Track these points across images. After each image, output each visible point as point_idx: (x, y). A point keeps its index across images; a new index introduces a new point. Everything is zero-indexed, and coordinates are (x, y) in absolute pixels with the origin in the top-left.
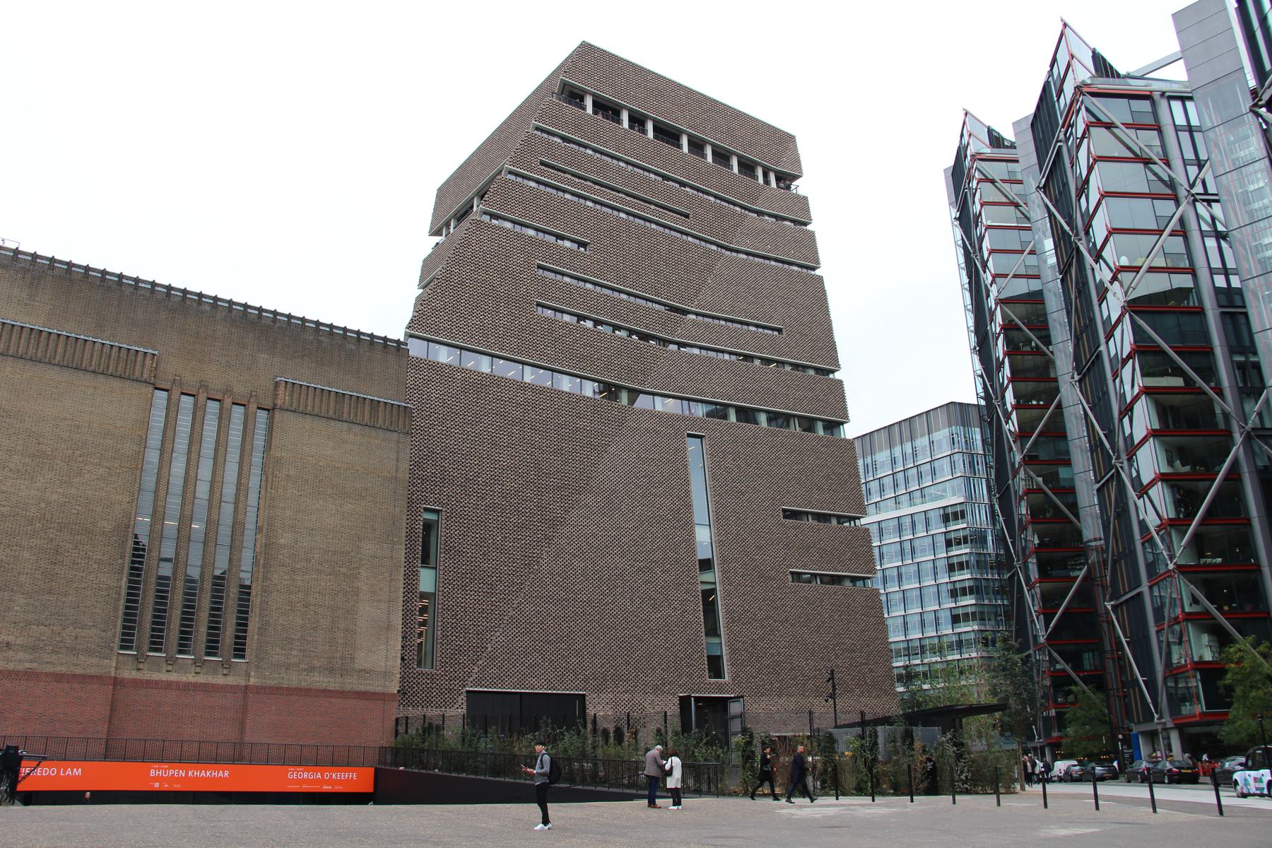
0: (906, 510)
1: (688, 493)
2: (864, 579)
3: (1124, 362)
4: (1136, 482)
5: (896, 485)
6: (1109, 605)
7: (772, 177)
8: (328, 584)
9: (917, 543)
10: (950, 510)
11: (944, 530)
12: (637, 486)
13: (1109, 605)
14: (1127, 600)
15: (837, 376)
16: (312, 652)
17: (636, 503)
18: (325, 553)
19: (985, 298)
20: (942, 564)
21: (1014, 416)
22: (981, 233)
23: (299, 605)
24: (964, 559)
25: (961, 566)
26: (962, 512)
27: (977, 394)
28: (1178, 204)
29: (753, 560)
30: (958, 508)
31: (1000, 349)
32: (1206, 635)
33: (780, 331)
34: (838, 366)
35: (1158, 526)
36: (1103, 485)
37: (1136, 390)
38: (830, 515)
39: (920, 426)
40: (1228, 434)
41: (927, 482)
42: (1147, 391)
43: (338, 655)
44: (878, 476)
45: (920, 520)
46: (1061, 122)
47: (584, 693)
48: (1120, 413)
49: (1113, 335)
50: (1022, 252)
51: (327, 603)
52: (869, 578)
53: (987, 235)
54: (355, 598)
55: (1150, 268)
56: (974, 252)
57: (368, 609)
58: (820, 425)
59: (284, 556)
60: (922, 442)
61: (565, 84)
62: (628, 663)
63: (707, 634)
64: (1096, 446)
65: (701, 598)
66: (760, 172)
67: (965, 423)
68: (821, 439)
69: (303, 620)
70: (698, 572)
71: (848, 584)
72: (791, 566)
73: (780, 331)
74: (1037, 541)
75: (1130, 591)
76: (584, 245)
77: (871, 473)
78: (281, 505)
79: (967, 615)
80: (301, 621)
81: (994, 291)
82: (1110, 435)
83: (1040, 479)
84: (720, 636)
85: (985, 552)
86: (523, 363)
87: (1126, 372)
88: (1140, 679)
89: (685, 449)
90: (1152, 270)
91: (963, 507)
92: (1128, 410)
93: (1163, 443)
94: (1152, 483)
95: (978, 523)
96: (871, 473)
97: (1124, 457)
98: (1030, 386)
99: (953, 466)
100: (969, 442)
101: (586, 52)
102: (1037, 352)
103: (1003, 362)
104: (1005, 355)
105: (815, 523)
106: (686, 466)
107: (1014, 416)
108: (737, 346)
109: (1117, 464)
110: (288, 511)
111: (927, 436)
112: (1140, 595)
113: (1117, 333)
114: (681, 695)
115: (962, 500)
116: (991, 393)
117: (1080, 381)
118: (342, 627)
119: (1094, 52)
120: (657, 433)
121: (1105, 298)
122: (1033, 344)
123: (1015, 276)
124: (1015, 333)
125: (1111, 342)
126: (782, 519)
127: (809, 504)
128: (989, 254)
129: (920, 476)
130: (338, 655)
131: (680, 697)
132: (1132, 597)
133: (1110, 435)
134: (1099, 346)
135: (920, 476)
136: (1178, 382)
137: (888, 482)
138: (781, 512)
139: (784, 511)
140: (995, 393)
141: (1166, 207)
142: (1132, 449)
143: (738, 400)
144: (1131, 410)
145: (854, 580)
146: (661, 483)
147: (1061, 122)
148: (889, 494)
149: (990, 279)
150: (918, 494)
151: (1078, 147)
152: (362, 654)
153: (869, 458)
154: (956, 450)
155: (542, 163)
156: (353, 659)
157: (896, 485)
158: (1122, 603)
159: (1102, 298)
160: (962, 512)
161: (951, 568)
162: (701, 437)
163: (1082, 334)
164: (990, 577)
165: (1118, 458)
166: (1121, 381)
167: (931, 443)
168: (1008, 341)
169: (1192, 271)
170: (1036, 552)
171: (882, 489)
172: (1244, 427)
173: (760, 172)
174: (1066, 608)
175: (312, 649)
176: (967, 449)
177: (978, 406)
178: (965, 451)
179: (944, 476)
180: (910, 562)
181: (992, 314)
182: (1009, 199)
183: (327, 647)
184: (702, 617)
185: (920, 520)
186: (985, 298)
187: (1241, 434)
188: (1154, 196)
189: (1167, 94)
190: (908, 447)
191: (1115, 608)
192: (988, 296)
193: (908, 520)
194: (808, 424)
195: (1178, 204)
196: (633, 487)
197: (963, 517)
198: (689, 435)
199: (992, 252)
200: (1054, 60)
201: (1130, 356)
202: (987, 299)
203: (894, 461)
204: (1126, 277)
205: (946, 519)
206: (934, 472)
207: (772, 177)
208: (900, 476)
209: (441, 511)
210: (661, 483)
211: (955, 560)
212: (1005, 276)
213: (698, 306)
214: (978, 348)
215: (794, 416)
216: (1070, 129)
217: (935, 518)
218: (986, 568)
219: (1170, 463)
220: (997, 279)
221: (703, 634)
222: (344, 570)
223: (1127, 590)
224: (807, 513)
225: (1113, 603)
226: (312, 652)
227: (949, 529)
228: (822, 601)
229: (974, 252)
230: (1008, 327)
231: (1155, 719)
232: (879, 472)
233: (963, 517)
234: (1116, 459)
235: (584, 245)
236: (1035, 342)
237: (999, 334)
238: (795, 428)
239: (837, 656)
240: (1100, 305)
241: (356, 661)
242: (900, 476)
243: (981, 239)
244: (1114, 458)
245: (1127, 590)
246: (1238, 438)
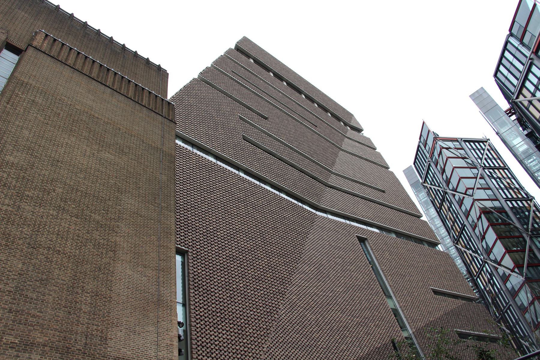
8: (73, 227)
16: (34, 316)
18: (72, 191)
23: (21, 242)
43: (80, 329)
51: (67, 250)
54: (111, 254)
57: (129, 272)
59: (9, 175)
69: (24, 264)
78: (17, 123)
80: (20, 266)
101: (245, 40)
110: (26, 133)
118: (89, 287)
130: (80, 329)
152: (119, 334)
155: (232, 71)
156: (104, 340)
175: (32, 312)
183: (61, 314)
209: (187, 251)
222: (98, 217)
226: (34, 316)
241: (111, 343)
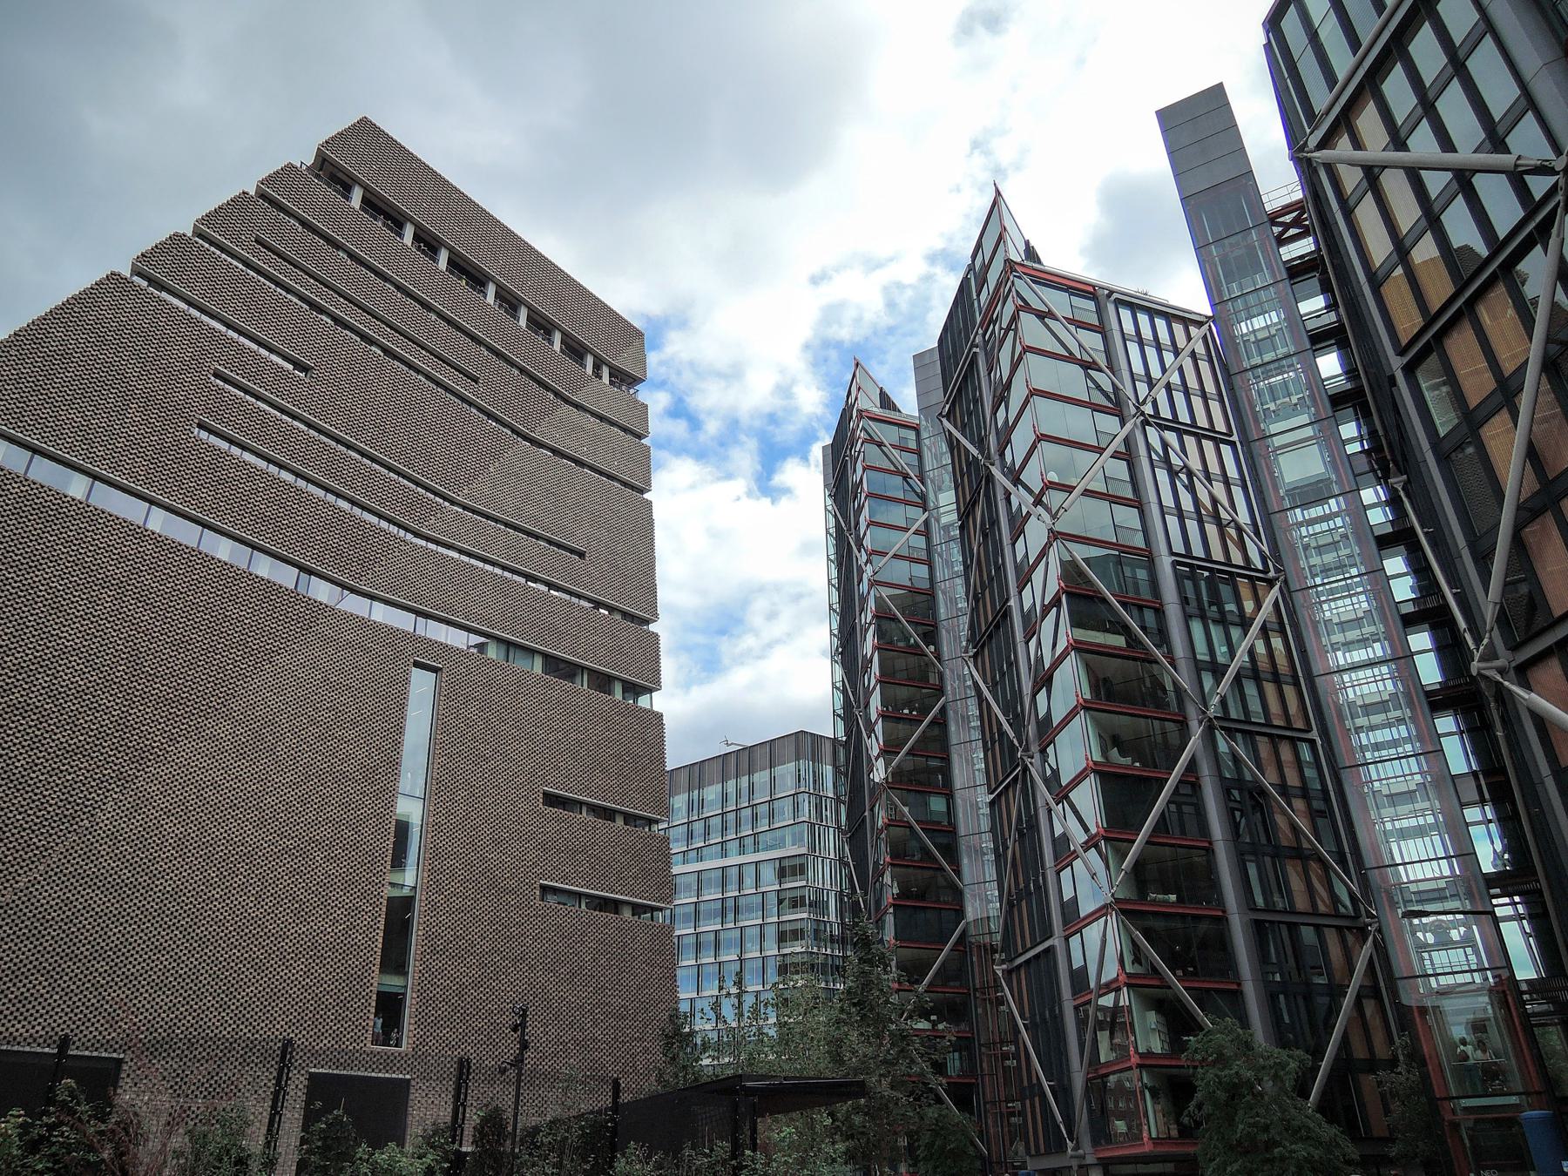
0: (734, 859)
1: (397, 744)
2: (653, 909)
3: (1046, 610)
4: (1053, 780)
5: (724, 829)
6: (999, 970)
7: (605, 372)
9: (742, 901)
10: (786, 863)
11: (777, 887)
12: (313, 721)
13: (999, 970)
14: (1028, 962)
15: (653, 627)
17: (305, 746)
19: (856, 583)
20: (771, 932)
21: (879, 728)
22: (859, 505)
24: (798, 926)
25: (797, 935)
26: (802, 866)
27: (834, 711)
28: (1123, 424)
29: (483, 859)
30: (797, 861)
31: (869, 643)
32: (1154, 1012)
33: (581, 555)
34: (656, 615)
35: (1086, 843)
36: (999, 795)
37: (1062, 645)
38: (615, 811)
39: (762, 757)
40: (1183, 725)
41: (763, 826)
42: (1078, 647)
44: (704, 816)
45: (749, 872)
46: (979, 320)
47: (122, 1056)
48: (1035, 683)
49: (1030, 580)
50: (906, 530)
52: (661, 909)
53: (866, 504)
55: (1086, 490)
56: (849, 530)
58: (618, 689)
60: (761, 777)
61: (324, 160)
62: (224, 1007)
63: (385, 968)
64: (993, 739)
65: (384, 909)
66: (590, 360)
67: (816, 758)
68: (616, 704)
70: (389, 867)
71: (627, 913)
72: (543, 877)
73: (581, 555)
74: (896, 891)
75: (1032, 948)
76: (305, 369)
77: (695, 812)
79: (796, 965)
81: (869, 570)
82: (1018, 721)
83: (906, 810)
84: (405, 974)
85: (826, 919)
86: (152, 502)
87: (1047, 626)
88: (1045, 1084)
89: (407, 681)
90: (1088, 493)
91: (803, 860)
92: (1044, 681)
93: (1096, 722)
94: (1077, 781)
95: (821, 882)
96: (695, 812)
97: (1035, 748)
98: (903, 693)
99: (796, 808)
100: (817, 779)
102: (915, 651)
103: (871, 661)
104: (875, 648)
105: (591, 818)
106: (402, 707)
107: (879, 728)
108: (515, 560)
109: (1025, 758)
111: (768, 770)
112: (1050, 951)
113: (1038, 576)
114: (313, 1070)
115: (804, 850)
116: (851, 710)
117: (975, 656)
119: (1027, 243)
120: (367, 651)
121: (1023, 531)
122: (912, 641)
123: (895, 556)
124: (886, 625)
125: (1027, 592)
126: (541, 806)
127: (586, 790)
128: (868, 527)
129: (755, 818)
131: (311, 1074)
132: (1037, 956)
133: (1018, 721)
134: (1008, 600)
135: (755, 818)
136: (1119, 641)
137: (716, 822)
138: (541, 795)
139: (546, 794)
140: (858, 701)
141: (1109, 423)
142: (1048, 731)
143: (504, 629)
144: (1051, 677)
145: (638, 909)
146: (355, 723)
147: (979, 320)
148: (716, 838)
149: (864, 558)
150: (749, 841)
151: (1002, 341)
153: (696, 792)
154: (802, 789)
157: (724, 829)
158: (1020, 966)
159: (1018, 531)
160: (802, 866)
161: (782, 938)
162: (435, 670)
163: (983, 593)
164: (829, 952)
165: (1027, 749)
166: (1039, 643)
167: (773, 780)
168: (880, 633)
169: (1138, 504)
170: (894, 905)
171: (707, 833)
172: (1204, 713)
173: (590, 360)
174: (943, 964)
176: (815, 789)
177: (835, 740)
178: (812, 791)
179: (784, 820)
180: (732, 925)
181: (863, 599)
182: (897, 468)
184: (381, 940)
185: (749, 872)
186: (856, 583)
187: (1200, 722)
188: (1096, 408)
189: (1115, 296)
190: (744, 780)
191: (1008, 973)
192: (860, 580)
193: (735, 871)
194: (603, 682)
195: (1123, 424)
196: (305, 721)
197: (802, 873)
198: (417, 665)
199: (870, 495)
200: (979, 246)
201: (1056, 602)
202: (859, 585)
203: (725, 798)
204: (1055, 498)
205: (782, 874)
206: (771, 815)
207: (605, 372)
208: (731, 817)
210: (355, 723)
211: (788, 927)
212: (884, 554)
213: (468, 496)
214: (840, 650)
215: (583, 668)
216: (992, 326)
217: (768, 873)
218: (825, 941)
219: (1104, 753)
220: (874, 557)
221: (376, 969)
223: (1029, 945)
224: (581, 803)
225: (1004, 966)
227: (785, 886)
228: (584, 934)
229: (849, 530)
230: (883, 616)
231: (1069, 1150)
232: (705, 810)
233: (802, 873)
234: (1023, 751)
235: (305, 369)
236: (915, 638)
237: (870, 624)
238: (583, 683)
239: (595, 1023)
240: (1013, 545)
242: (731, 817)
243: (861, 508)
244: (1020, 749)
245: (1029, 945)
246: (1197, 732)
